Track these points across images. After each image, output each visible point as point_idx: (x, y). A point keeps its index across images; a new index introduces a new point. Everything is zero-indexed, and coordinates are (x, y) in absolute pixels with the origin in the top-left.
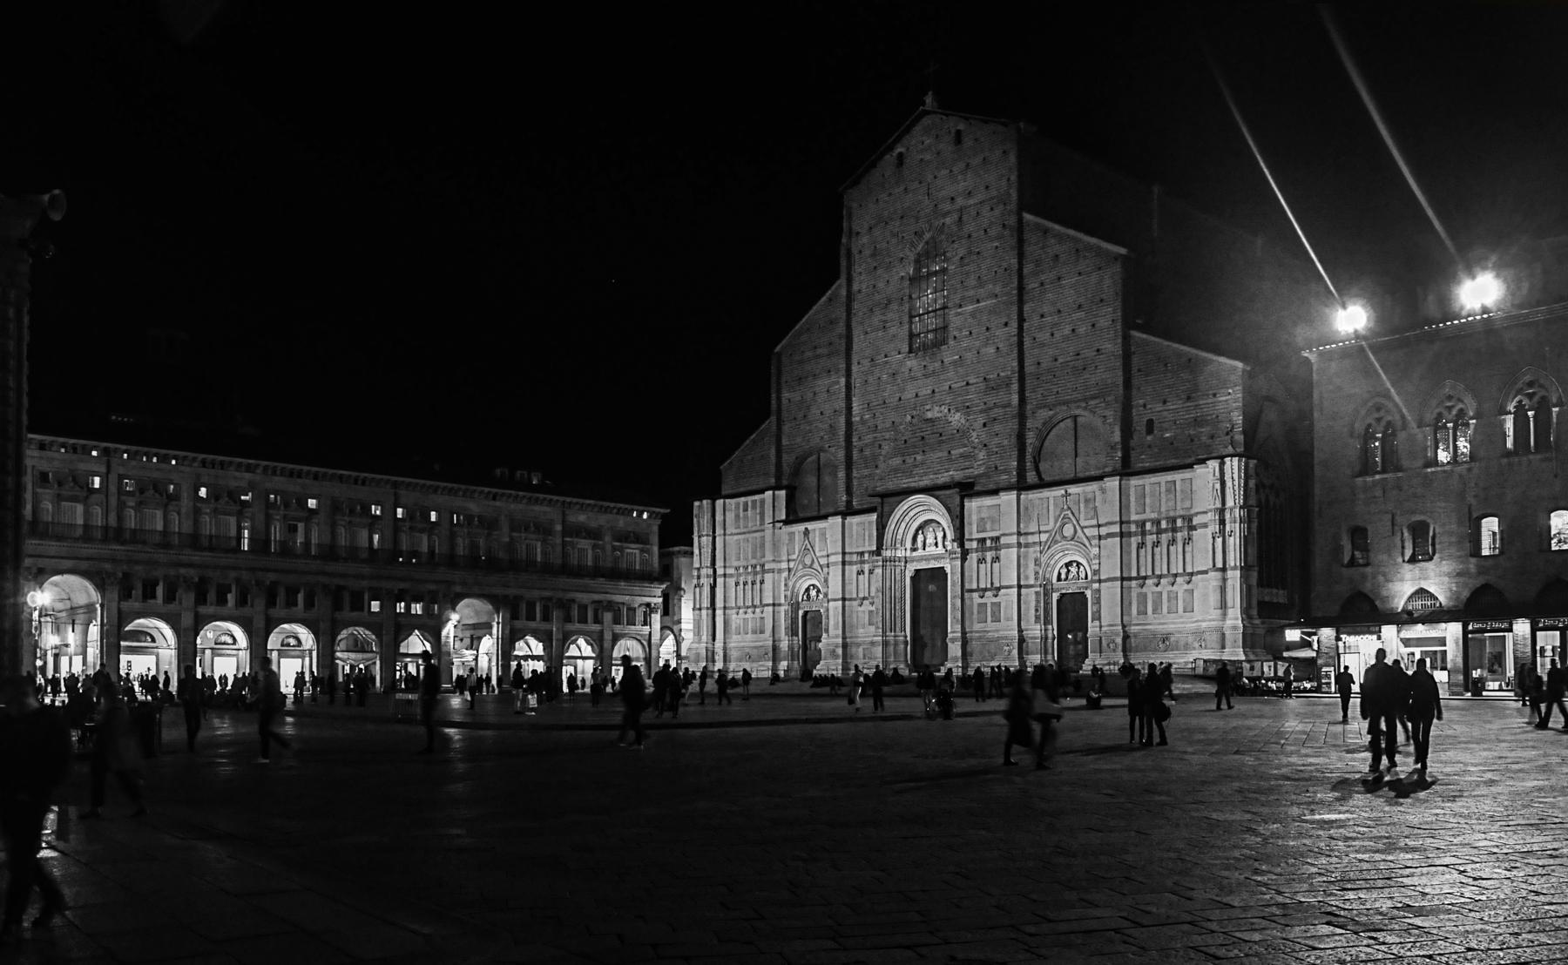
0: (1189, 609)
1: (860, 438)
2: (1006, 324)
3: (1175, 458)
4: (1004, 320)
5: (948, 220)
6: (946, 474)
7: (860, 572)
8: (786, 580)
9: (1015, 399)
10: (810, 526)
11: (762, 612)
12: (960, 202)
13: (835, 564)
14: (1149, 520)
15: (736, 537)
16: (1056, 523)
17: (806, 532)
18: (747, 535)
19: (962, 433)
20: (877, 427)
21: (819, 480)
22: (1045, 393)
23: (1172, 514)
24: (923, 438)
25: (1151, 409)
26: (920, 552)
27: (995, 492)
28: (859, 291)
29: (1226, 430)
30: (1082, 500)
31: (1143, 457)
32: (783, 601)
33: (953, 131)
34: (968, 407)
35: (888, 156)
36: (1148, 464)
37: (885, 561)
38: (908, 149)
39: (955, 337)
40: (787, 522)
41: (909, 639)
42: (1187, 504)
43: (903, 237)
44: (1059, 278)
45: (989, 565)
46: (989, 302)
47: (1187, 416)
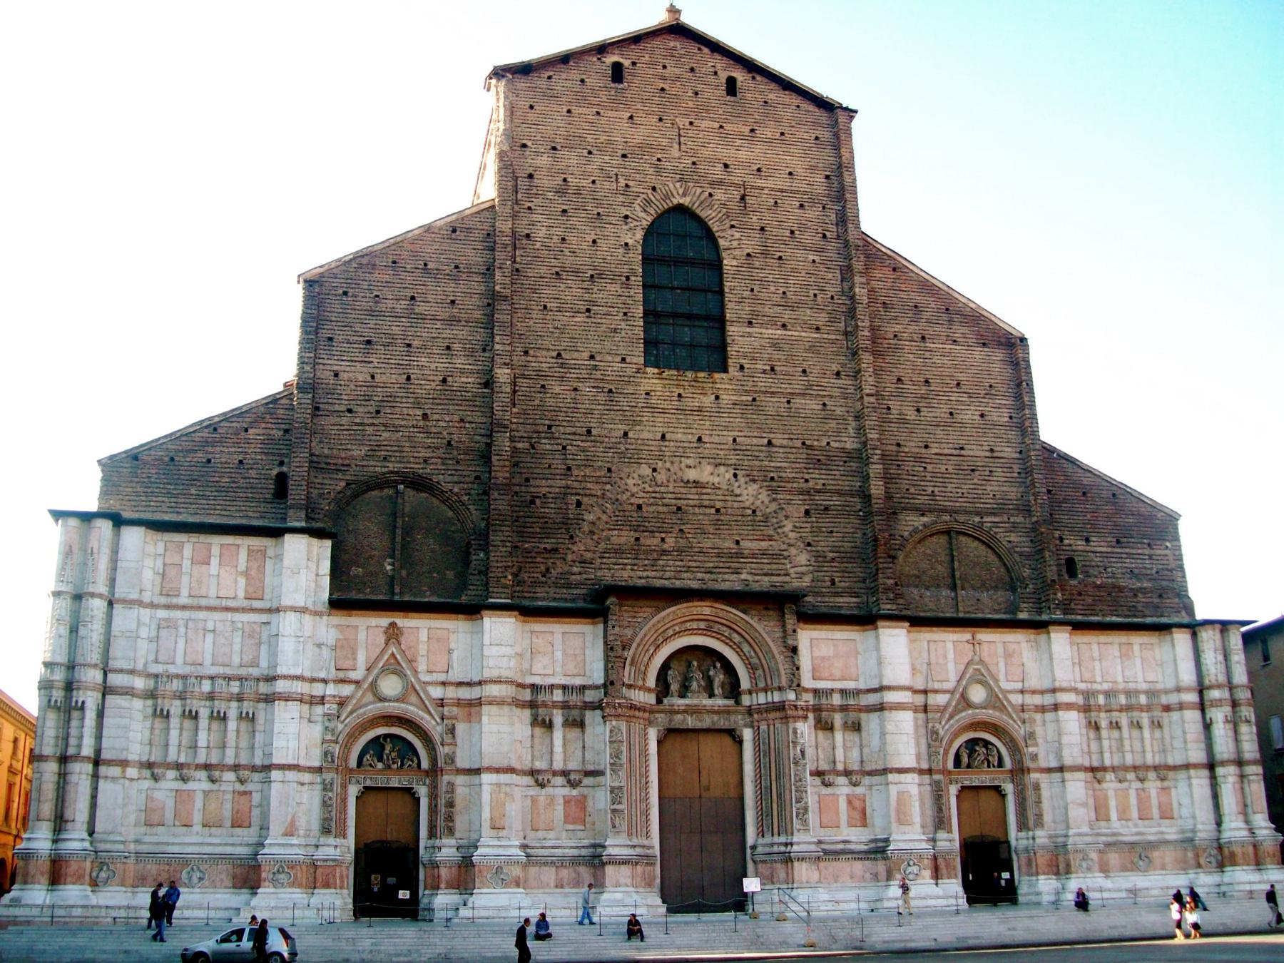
0: (1166, 814)
1: (527, 480)
2: (838, 374)
3: (1117, 616)
4: (835, 368)
5: (719, 195)
6: (734, 577)
10: (405, 622)
12: (738, 176)
13: (499, 702)
15: (162, 614)
17: (393, 634)
18: (202, 615)
20: (569, 469)
22: (912, 490)
23: (1131, 686)
24: (679, 509)
28: (528, 236)
30: (1000, 650)
31: (1073, 606)
33: (723, 76)
34: (772, 479)
35: (595, 59)
38: (634, 64)
39: (742, 367)
41: (658, 854)
42: (1151, 677)
43: (627, 186)
44: (923, 338)
46: (803, 334)
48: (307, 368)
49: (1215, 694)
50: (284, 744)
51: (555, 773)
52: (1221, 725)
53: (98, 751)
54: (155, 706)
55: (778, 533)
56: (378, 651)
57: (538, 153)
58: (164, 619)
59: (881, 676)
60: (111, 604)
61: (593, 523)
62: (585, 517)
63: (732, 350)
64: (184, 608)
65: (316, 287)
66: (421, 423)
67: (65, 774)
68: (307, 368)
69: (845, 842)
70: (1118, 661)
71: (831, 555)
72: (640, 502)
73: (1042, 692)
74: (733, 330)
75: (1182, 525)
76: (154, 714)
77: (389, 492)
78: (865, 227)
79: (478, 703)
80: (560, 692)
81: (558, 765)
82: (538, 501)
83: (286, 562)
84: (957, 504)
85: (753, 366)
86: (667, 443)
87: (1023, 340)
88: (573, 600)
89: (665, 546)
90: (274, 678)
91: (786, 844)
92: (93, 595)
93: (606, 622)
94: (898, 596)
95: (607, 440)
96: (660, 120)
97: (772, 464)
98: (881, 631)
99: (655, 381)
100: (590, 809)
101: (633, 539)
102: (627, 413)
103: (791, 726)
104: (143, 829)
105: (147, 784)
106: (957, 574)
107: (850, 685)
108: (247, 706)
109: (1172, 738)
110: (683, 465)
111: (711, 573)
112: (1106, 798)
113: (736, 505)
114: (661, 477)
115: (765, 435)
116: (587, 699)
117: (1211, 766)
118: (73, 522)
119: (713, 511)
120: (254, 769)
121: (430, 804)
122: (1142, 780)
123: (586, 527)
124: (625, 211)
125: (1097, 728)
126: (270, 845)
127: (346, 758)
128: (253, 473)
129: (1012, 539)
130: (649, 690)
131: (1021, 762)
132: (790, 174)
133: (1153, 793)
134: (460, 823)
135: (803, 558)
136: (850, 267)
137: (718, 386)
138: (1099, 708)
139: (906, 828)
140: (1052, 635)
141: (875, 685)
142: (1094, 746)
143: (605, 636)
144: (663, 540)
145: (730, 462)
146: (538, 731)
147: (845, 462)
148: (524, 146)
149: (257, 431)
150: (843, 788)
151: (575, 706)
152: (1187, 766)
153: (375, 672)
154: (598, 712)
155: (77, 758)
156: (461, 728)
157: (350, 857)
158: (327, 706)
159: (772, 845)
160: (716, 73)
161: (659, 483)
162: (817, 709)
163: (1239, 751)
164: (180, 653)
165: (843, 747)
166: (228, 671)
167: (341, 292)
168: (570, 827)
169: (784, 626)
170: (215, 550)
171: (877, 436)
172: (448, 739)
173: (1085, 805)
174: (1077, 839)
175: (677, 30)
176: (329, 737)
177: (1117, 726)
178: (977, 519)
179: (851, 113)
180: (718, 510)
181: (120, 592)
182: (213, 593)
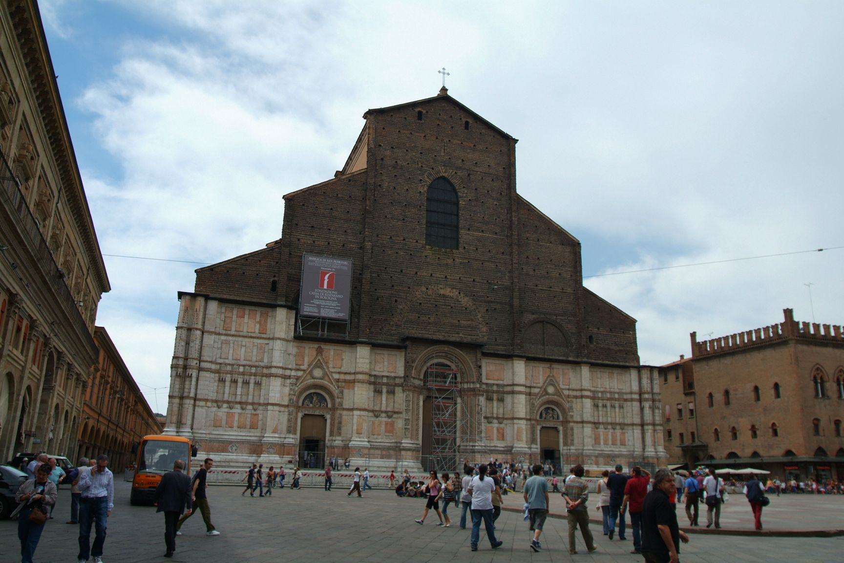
0: (623, 443)
1: (376, 290)
2: (503, 253)
4: (502, 250)
6: (457, 335)
10: (323, 346)
15: (223, 338)
17: (320, 351)
18: (240, 339)
20: (393, 286)
22: (530, 304)
23: (612, 390)
24: (436, 306)
28: (380, 185)
30: (561, 372)
32: (286, 402)
33: (464, 120)
39: (464, 248)
42: (620, 387)
43: (422, 166)
45: (495, 403)
49: (646, 396)
50: (273, 395)
51: (382, 412)
52: (648, 409)
53: (196, 395)
54: (220, 377)
57: (386, 150)
58: (225, 340)
59: (513, 380)
60: (203, 333)
61: (402, 310)
63: (461, 241)
64: (233, 336)
65: (290, 200)
67: (182, 404)
69: (495, 446)
70: (608, 379)
72: (421, 302)
73: (576, 390)
74: (462, 232)
75: (637, 325)
76: (219, 380)
78: (518, 192)
79: (354, 381)
80: (386, 378)
81: (383, 409)
82: (380, 299)
83: (277, 319)
87: (579, 244)
88: (392, 341)
89: (430, 321)
90: (271, 367)
91: (473, 446)
92: (197, 329)
93: (406, 351)
94: (522, 347)
96: (437, 138)
98: (514, 361)
100: (395, 427)
103: (477, 398)
104: (213, 428)
105: (214, 409)
106: (545, 339)
107: (501, 382)
108: (258, 379)
109: (627, 412)
110: (439, 288)
112: (599, 434)
113: (459, 305)
114: (430, 292)
116: (397, 382)
117: (642, 425)
119: (450, 307)
120: (260, 404)
121: (331, 422)
122: (614, 429)
123: (399, 311)
124: (420, 178)
125: (597, 406)
126: (267, 437)
127: (298, 401)
128: (262, 280)
130: (421, 380)
131: (566, 418)
132: (489, 166)
133: (618, 434)
134: (343, 430)
135: (484, 329)
136: (511, 208)
138: (599, 398)
139: (520, 442)
140: (582, 367)
141: (510, 383)
142: (596, 413)
143: (405, 355)
148: (380, 146)
149: (265, 262)
150: (495, 424)
151: (392, 385)
152: (633, 425)
153: (312, 367)
154: (401, 388)
155: (188, 397)
156: (346, 391)
157: (298, 442)
158: (291, 380)
159: (467, 446)
160: (461, 119)
161: (429, 294)
163: (654, 420)
164: (231, 355)
165: (496, 408)
166: (251, 363)
167: (301, 204)
168: (387, 434)
169: (476, 357)
170: (247, 312)
172: (340, 395)
173: (591, 437)
174: (587, 451)
175: (444, 98)
176: (292, 393)
177: (604, 406)
178: (555, 317)
179: (516, 141)
181: (207, 328)
182: (245, 330)
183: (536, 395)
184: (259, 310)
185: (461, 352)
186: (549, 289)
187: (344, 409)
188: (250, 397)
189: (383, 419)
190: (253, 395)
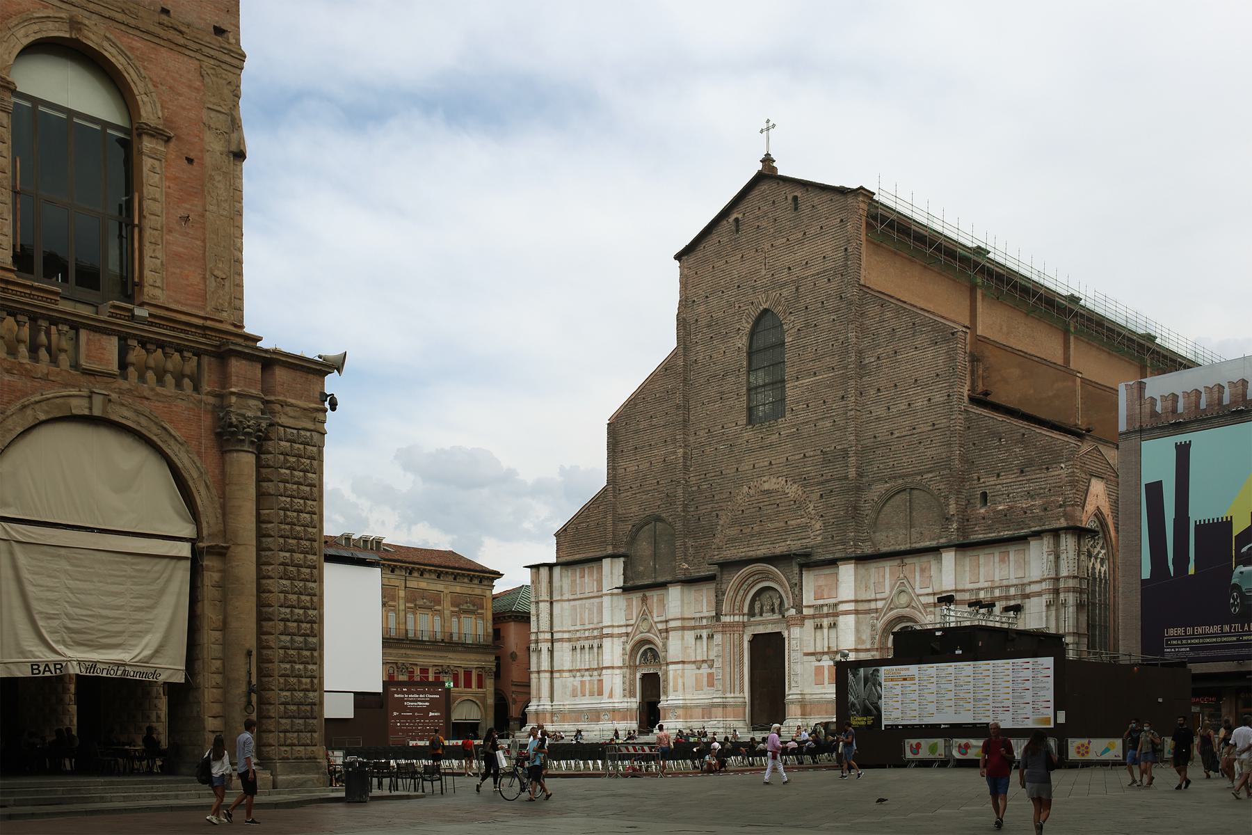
1: (697, 507)
6: (783, 544)
7: (699, 638)
8: (624, 643)
9: (852, 473)
10: (648, 594)
11: (600, 675)
13: (675, 629)
14: (982, 589)
15: (572, 603)
16: (891, 592)
18: (584, 601)
19: (798, 504)
20: (714, 496)
21: (655, 547)
23: (1005, 583)
25: (984, 482)
26: (758, 618)
27: (833, 563)
29: (1058, 504)
30: (917, 569)
31: (976, 529)
36: (981, 536)
37: (725, 625)
39: (792, 410)
40: (626, 589)
47: (1020, 490)
48: (610, 471)
55: (806, 513)
56: (639, 609)
60: (551, 603)
62: (719, 523)
66: (656, 487)
68: (610, 471)
70: (997, 565)
71: (833, 520)
77: (650, 525)
79: (667, 631)
82: (701, 518)
84: (908, 470)
85: (797, 408)
86: (755, 470)
92: (541, 601)
95: (728, 475)
97: (805, 469)
99: (750, 433)
101: (739, 531)
102: (738, 457)
106: (908, 518)
110: (762, 482)
111: (774, 543)
113: (786, 500)
114: (752, 492)
115: (802, 451)
118: (534, 570)
129: (940, 487)
130: (744, 615)
135: (818, 525)
137: (780, 426)
144: (752, 528)
145: (784, 474)
146: (698, 642)
147: (844, 457)
153: (639, 619)
162: (813, 617)
170: (586, 572)
171: (853, 438)
178: (919, 478)
180: (778, 505)
183: (876, 610)
184: (595, 565)
185: (776, 570)
186: (909, 433)
187: (667, 664)
188: (596, 662)
189: (705, 670)
190: (598, 660)
